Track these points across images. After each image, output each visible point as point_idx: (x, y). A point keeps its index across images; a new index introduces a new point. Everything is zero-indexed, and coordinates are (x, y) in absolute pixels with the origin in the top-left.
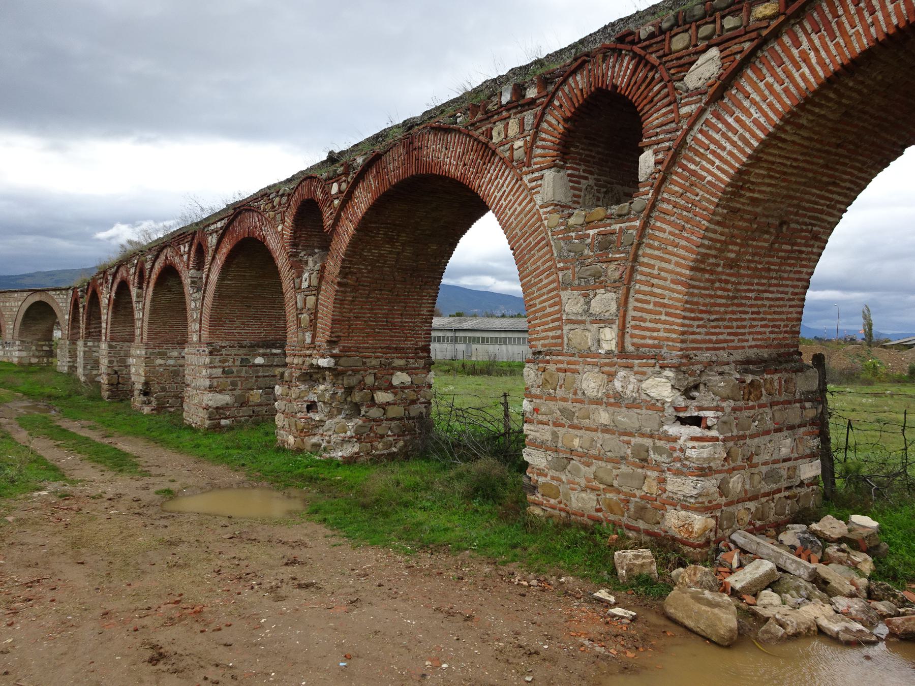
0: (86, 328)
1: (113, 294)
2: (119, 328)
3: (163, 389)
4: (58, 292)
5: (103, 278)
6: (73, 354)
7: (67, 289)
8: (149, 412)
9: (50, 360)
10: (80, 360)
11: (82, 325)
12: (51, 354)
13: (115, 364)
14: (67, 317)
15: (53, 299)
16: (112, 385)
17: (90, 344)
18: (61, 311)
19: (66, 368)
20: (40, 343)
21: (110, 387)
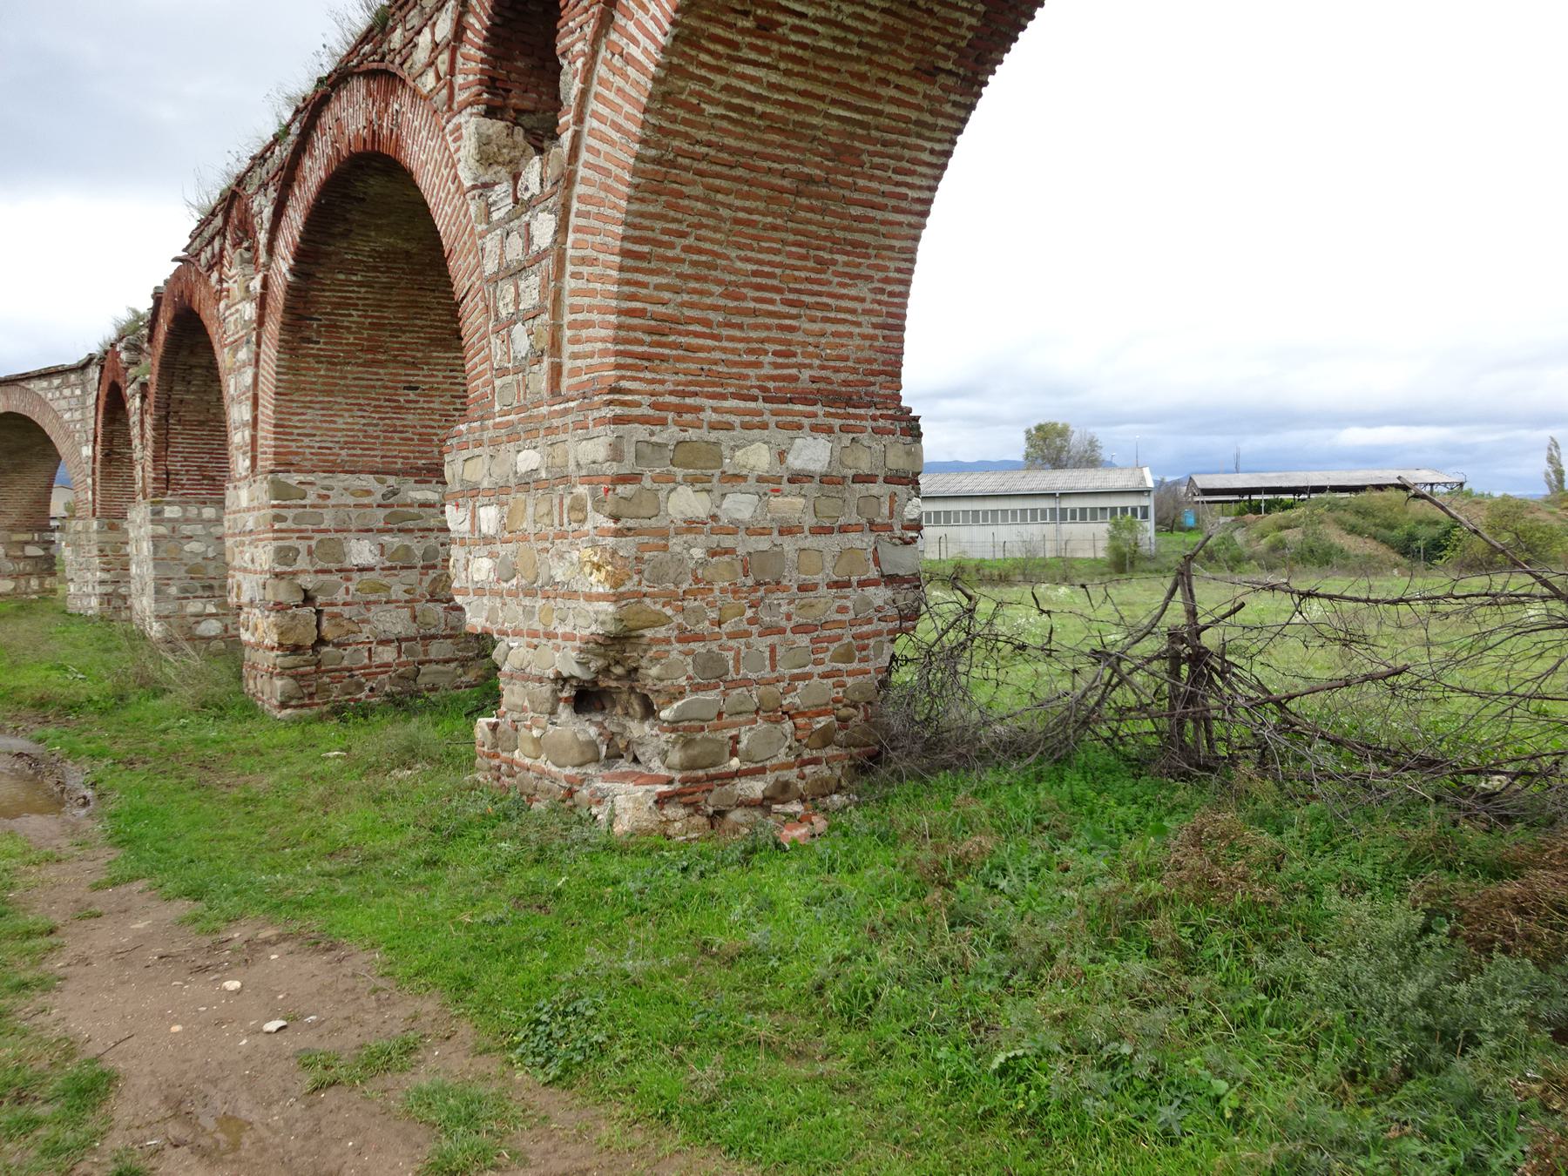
0: (156, 459)
1: (283, 265)
2: (310, 413)
3: (712, 673)
4: (56, 382)
5: (221, 232)
6: (116, 562)
7: (83, 367)
8: (648, 818)
9: (48, 582)
10: (142, 569)
11: (142, 452)
12: (48, 565)
13: (302, 563)
14: (87, 451)
15: (43, 403)
16: (296, 649)
17: (172, 512)
18: (69, 435)
19: (94, 602)
20: (16, 537)
21: (290, 660)
